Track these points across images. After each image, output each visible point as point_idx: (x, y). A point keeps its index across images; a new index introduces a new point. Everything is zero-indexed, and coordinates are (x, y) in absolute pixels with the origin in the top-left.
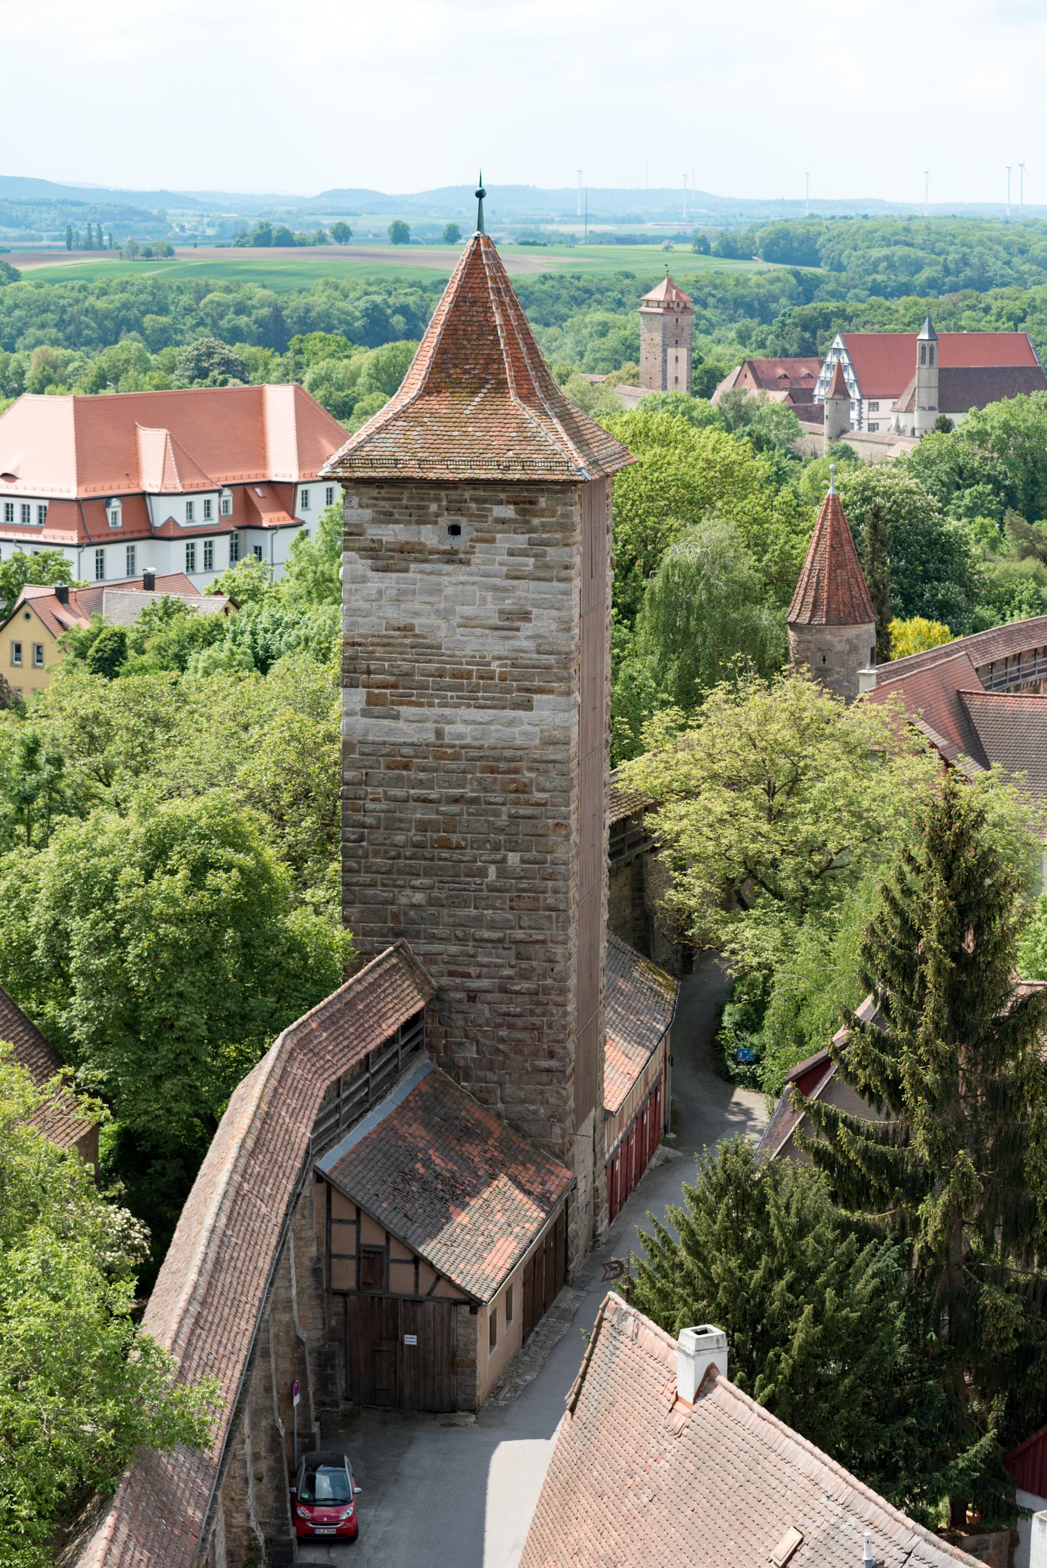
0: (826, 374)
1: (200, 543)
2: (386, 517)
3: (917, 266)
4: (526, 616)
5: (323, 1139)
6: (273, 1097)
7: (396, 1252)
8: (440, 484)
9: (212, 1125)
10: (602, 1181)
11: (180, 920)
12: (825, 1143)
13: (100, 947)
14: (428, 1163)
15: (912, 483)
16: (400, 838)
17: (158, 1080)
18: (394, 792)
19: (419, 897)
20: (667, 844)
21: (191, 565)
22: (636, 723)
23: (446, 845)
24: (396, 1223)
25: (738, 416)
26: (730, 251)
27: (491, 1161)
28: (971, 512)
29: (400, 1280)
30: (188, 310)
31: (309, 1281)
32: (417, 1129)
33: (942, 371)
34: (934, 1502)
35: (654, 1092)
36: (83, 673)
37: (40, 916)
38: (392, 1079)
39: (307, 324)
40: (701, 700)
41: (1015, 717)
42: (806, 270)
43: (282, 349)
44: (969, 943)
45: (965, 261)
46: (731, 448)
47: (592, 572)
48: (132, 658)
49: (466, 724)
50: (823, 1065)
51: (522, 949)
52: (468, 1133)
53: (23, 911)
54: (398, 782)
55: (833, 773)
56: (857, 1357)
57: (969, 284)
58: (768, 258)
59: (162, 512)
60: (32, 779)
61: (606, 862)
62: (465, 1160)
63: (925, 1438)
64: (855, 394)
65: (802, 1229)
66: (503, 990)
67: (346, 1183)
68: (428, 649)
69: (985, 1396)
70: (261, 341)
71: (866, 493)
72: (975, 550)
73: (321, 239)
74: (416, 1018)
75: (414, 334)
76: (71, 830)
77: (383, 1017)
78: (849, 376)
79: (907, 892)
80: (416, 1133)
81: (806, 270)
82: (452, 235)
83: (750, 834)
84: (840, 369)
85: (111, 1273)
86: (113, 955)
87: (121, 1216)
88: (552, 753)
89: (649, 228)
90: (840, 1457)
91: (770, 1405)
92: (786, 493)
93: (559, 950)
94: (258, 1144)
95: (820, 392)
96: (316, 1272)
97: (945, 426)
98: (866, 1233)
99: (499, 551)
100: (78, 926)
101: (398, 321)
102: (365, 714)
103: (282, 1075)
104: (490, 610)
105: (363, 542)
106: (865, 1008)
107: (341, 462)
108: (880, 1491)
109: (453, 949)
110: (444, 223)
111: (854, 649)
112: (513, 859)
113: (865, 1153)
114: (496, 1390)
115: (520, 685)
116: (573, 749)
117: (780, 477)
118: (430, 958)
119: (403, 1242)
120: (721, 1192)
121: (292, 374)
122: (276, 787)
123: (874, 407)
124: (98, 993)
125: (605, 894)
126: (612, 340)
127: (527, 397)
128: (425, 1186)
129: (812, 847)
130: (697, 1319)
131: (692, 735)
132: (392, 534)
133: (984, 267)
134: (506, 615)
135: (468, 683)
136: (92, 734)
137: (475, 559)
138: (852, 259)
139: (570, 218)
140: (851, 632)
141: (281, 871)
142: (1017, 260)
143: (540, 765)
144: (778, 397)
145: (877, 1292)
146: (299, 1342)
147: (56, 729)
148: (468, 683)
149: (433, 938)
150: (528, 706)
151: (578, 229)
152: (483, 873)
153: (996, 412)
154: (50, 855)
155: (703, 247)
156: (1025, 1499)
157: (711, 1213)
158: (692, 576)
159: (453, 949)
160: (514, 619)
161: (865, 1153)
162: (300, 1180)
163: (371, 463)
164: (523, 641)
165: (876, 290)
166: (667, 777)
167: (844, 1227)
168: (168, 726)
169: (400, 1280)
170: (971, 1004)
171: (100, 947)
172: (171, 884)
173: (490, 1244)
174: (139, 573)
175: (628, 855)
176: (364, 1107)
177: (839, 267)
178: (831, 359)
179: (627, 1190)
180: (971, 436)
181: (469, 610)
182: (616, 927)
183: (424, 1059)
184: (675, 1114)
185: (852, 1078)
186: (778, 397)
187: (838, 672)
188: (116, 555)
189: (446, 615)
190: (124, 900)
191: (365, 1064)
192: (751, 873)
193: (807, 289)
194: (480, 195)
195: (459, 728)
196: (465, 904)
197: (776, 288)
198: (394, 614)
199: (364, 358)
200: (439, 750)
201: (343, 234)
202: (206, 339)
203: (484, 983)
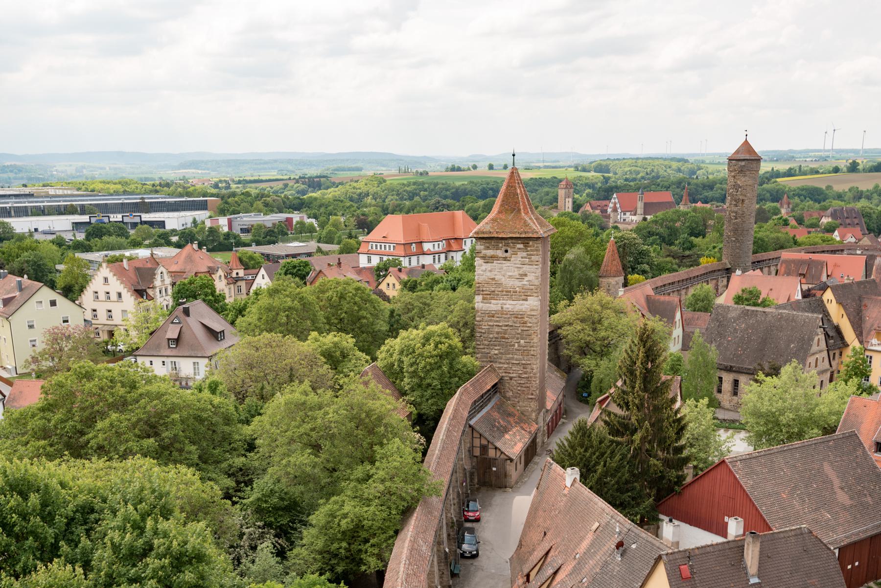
0: (611, 205)
1: (437, 256)
2: (488, 248)
3: (638, 173)
4: (526, 275)
5: (471, 416)
6: (458, 404)
7: (490, 446)
8: (502, 239)
9: (441, 411)
10: (546, 428)
11: (432, 357)
12: (607, 419)
13: (411, 365)
14: (499, 423)
15: (634, 236)
16: (491, 336)
17: (427, 400)
18: (491, 324)
19: (496, 352)
20: (564, 338)
21: (434, 261)
22: (556, 305)
24: (490, 438)
25: (585, 218)
26: (584, 170)
28: (652, 244)
29: (492, 453)
30: (433, 190)
31: (467, 453)
33: (645, 204)
34: (636, 516)
35: (560, 405)
37: (396, 356)
38: (489, 400)
39: (465, 193)
40: (573, 298)
41: (663, 302)
42: (606, 175)
43: (459, 201)
44: (650, 365)
45: (653, 171)
46: (583, 227)
47: (544, 263)
48: (419, 288)
49: (510, 305)
50: (608, 397)
51: (525, 366)
52: (510, 415)
53: (391, 355)
54: (491, 321)
55: (610, 317)
56: (615, 476)
57: (653, 177)
58: (595, 171)
59: (427, 247)
60: (393, 320)
61: (548, 342)
62: (509, 422)
63: (633, 499)
64: (619, 211)
65: (601, 442)
67: (477, 428)
69: (650, 488)
70: (453, 199)
71: (622, 238)
72: (653, 255)
73: (469, 169)
74: (496, 384)
75: (495, 196)
76: (403, 333)
77: (487, 384)
78: (618, 206)
79: (632, 351)
80: (496, 415)
81: (606, 175)
82: (505, 167)
83: (587, 335)
84: (615, 204)
85: (415, 450)
86: (416, 366)
87: (418, 436)
89: (561, 164)
90: (610, 503)
91: (591, 488)
92: (598, 239)
94: (454, 417)
95: (609, 210)
96: (469, 451)
98: (618, 443)
99: (519, 256)
100: (404, 359)
101: (491, 192)
103: (460, 399)
104: (516, 273)
105: (481, 255)
106: (619, 383)
107: (475, 233)
108: (621, 513)
109: (506, 366)
110: (503, 164)
111: (617, 283)
112: (522, 342)
113: (618, 422)
114: (517, 483)
115: (525, 295)
116: (539, 312)
117: (597, 235)
118: (500, 368)
119: (492, 444)
120: (578, 432)
121: (461, 208)
122: (458, 322)
123: (625, 214)
124: (411, 378)
125: (547, 351)
126: (549, 197)
127: (527, 213)
129: (604, 339)
130: (571, 465)
131: (571, 308)
132: (490, 252)
133: (658, 172)
134: (521, 275)
135: (510, 294)
136: (408, 308)
138: (619, 171)
139: (538, 161)
140: (617, 279)
141: (460, 345)
142: (668, 170)
144: (597, 212)
145: (621, 460)
147: (397, 307)
148: (510, 294)
149: (500, 363)
150: (526, 300)
151: (541, 165)
152: (514, 345)
153: (660, 214)
154: (398, 340)
155: (576, 168)
156: (661, 517)
157: (576, 438)
158: (570, 262)
159: (506, 366)
161: (618, 422)
162: (465, 427)
163: (483, 233)
165: (626, 180)
166: (564, 319)
167: (612, 442)
168: (429, 305)
169: (492, 453)
170: (649, 382)
171: (411, 365)
172: (430, 347)
173: (516, 444)
174: (420, 264)
175: (553, 341)
176: (482, 407)
177: (615, 174)
178: (613, 200)
179: (553, 431)
180: (653, 221)
181: (510, 274)
182: (550, 360)
183: (498, 395)
184: (566, 411)
185: (615, 402)
186: (597, 212)
187: (613, 290)
188: (414, 259)
190: (417, 352)
191: (482, 396)
192: (587, 346)
193: (607, 180)
194: (514, 155)
195: (507, 306)
197: (596, 181)
198: (489, 274)
199: (481, 203)
200: (502, 312)
201: (475, 167)
202: (437, 198)
203: (514, 375)
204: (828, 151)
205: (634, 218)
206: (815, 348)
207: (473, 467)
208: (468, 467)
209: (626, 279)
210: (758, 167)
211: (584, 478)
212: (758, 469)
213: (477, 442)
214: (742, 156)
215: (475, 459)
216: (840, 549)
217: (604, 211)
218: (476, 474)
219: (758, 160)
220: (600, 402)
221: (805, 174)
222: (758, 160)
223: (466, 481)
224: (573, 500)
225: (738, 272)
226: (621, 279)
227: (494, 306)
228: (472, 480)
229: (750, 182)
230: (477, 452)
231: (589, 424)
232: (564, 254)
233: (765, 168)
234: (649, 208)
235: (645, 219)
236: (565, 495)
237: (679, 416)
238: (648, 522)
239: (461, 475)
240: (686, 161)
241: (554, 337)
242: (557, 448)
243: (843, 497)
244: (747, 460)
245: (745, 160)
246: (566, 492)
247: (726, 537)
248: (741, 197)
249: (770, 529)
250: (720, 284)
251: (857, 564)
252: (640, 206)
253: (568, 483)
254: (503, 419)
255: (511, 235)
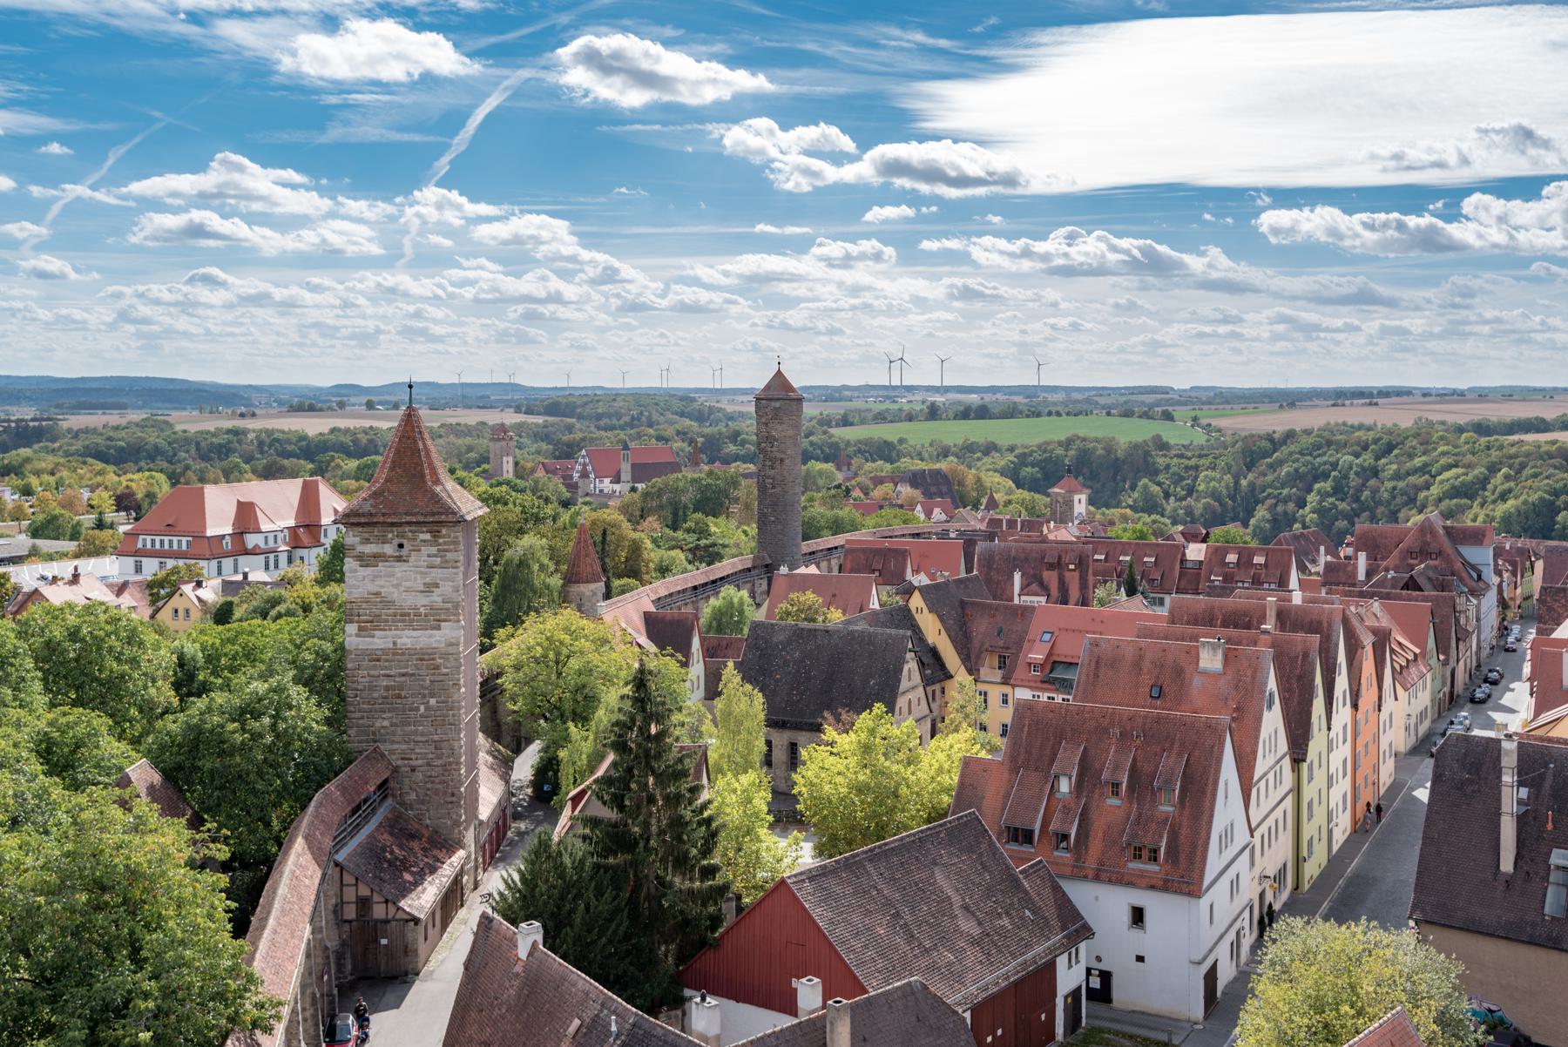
0: (578, 467)
1: (272, 556)
2: (367, 541)
3: (619, 416)
4: (437, 586)
7: (376, 898)
8: (393, 524)
14: (392, 853)
16: (376, 695)
18: (375, 673)
19: (386, 723)
23: (399, 697)
27: (424, 850)
31: (332, 917)
32: (386, 836)
36: (210, 624)
38: (374, 811)
43: (312, 461)
47: (468, 563)
49: (409, 638)
51: (437, 745)
54: (375, 667)
61: (478, 700)
66: (428, 765)
68: (387, 603)
74: (385, 782)
78: (589, 468)
84: (585, 465)
88: (450, 650)
93: (456, 744)
95: (576, 475)
96: (335, 912)
97: (633, 490)
102: (358, 635)
103: (317, 815)
105: (355, 553)
109: (404, 747)
111: (595, 594)
112: (433, 701)
115: (435, 618)
118: (392, 752)
128: (391, 864)
132: (369, 549)
135: (408, 618)
137: (412, 559)
140: (593, 586)
143: (445, 656)
146: (327, 948)
148: (408, 618)
150: (438, 628)
152: (418, 709)
153: (658, 481)
156: (688, 992)
159: (404, 747)
160: (430, 587)
163: (358, 515)
164: (436, 598)
169: (379, 911)
178: (581, 460)
181: (408, 584)
183: (389, 801)
189: (396, 586)
191: (358, 807)
195: (405, 640)
196: (409, 724)
198: (372, 587)
200: (395, 652)
204: (896, 388)
205: (617, 487)
206: (904, 684)
207: (343, 944)
208: (333, 944)
209: (608, 586)
210: (800, 410)
211: (551, 940)
212: (838, 890)
213: (350, 894)
214: (776, 394)
215: (347, 927)
216: (975, 1011)
217: (567, 478)
218: (348, 955)
219: (800, 400)
220: (573, 799)
221: (863, 422)
222: (800, 400)
223: (329, 973)
224: (534, 980)
225: (784, 570)
226: (600, 586)
227: (380, 641)
228: (340, 967)
229: (790, 433)
230: (350, 912)
231: (556, 839)
232: (498, 551)
233: (810, 410)
234: (640, 472)
235: (633, 490)
236: (517, 975)
237: (706, 814)
238: (667, 1000)
239: (320, 960)
240: (693, 400)
241: (490, 688)
242: (502, 887)
243: (967, 926)
244: (812, 876)
245: (779, 398)
246: (518, 969)
247: (793, 1012)
248: (779, 456)
249: (866, 992)
250: (758, 590)
251: (999, 1032)
252: (626, 470)
253: (523, 953)
254: (401, 847)
255: (408, 519)
